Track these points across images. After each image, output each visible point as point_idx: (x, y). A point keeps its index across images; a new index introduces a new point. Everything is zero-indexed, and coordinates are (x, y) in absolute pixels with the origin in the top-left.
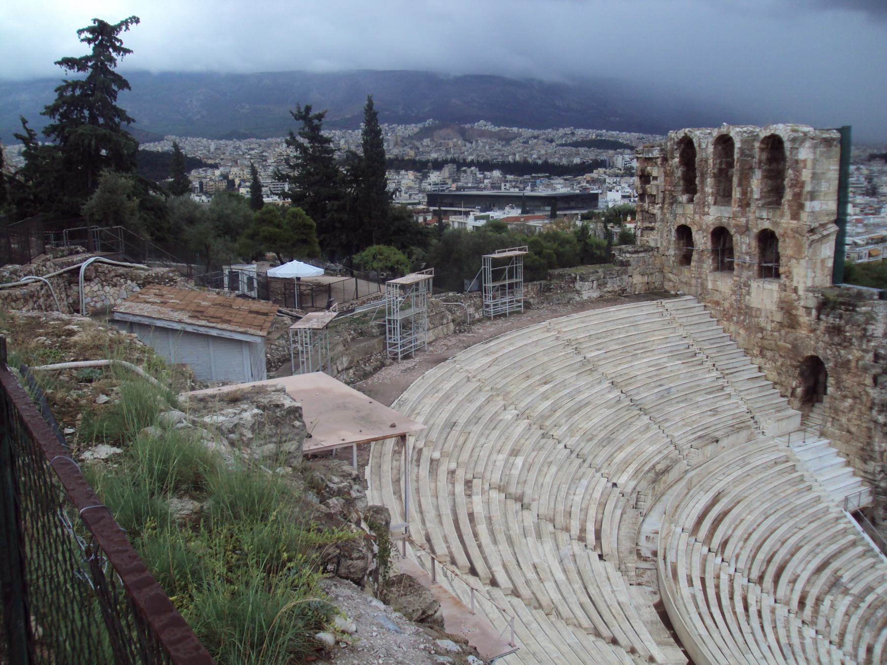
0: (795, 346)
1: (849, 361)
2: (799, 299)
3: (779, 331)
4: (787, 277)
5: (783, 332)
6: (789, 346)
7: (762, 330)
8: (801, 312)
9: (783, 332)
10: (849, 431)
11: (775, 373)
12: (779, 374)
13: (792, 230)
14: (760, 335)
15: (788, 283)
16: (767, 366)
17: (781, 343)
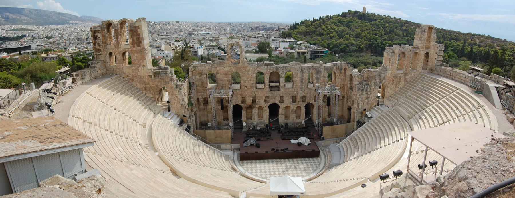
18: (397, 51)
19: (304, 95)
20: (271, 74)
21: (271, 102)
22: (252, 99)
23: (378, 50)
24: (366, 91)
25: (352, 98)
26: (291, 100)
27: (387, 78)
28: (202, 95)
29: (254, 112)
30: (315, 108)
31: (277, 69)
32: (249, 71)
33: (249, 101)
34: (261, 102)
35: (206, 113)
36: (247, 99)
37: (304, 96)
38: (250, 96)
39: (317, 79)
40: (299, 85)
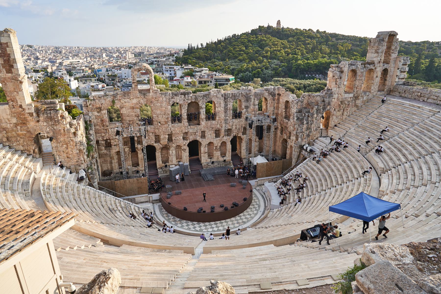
0: (29, 132)
1: (60, 130)
2: (24, 110)
3: (16, 127)
4: (12, 101)
5: (19, 127)
6: (25, 132)
7: (4, 129)
8: (27, 115)
9: (19, 127)
10: (68, 158)
11: (21, 147)
12: (23, 146)
13: (9, 78)
14: (5, 132)
15: (14, 104)
16: (14, 144)
17: (20, 132)
18: (346, 69)
19: (229, 128)
20: (189, 104)
21: (191, 138)
22: (167, 136)
23: (322, 70)
24: (307, 120)
25: (289, 129)
26: (214, 135)
27: (332, 104)
28: (103, 136)
29: (171, 152)
30: (243, 142)
31: (196, 98)
32: (162, 102)
33: (164, 140)
34: (179, 140)
35: (108, 159)
36: (162, 137)
37: (228, 129)
38: (164, 134)
39: (247, 107)
40: (223, 116)
